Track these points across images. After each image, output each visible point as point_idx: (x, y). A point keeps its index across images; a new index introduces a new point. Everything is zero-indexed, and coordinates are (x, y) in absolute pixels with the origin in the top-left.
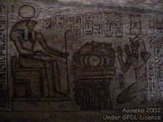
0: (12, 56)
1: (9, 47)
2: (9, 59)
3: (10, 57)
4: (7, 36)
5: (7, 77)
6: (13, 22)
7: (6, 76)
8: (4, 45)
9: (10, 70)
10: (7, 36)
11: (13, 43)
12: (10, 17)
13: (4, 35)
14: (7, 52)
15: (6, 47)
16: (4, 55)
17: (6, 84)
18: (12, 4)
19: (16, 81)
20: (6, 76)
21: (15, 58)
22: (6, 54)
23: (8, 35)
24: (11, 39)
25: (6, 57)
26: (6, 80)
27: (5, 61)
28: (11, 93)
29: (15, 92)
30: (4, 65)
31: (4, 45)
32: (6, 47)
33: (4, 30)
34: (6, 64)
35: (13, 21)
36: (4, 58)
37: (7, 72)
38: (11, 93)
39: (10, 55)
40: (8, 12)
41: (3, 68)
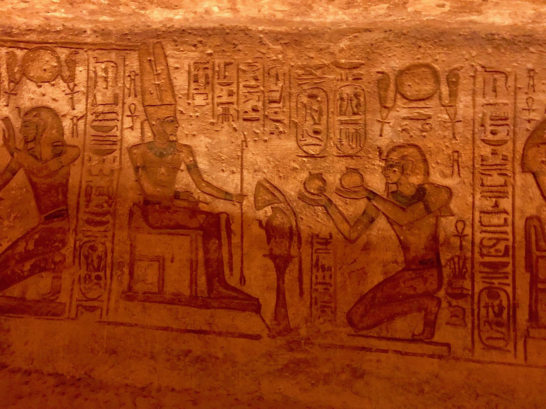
0: (528, 215)
1: (518, 191)
2: (520, 224)
3: (521, 217)
4: (513, 158)
5: (514, 272)
6: (529, 121)
7: (509, 269)
8: (505, 185)
9: (521, 254)
10: (513, 158)
11: (530, 178)
12: (521, 104)
13: (505, 158)
14: (513, 205)
15: (510, 190)
16: (506, 212)
17: (509, 289)
18: (530, 66)
19: (540, 286)
20: (509, 269)
21: (536, 223)
22: (510, 210)
23: (518, 156)
24: (525, 169)
25: (510, 218)
26: (509, 281)
27: (509, 229)
28: (523, 315)
29: (533, 316)
30: (507, 240)
31: (505, 185)
32: (510, 190)
33: (505, 142)
34: (510, 237)
35: (533, 115)
36: (506, 220)
37: (514, 257)
38: (523, 315)
39: (522, 212)
40: (517, 90)
41: (501, 246)
